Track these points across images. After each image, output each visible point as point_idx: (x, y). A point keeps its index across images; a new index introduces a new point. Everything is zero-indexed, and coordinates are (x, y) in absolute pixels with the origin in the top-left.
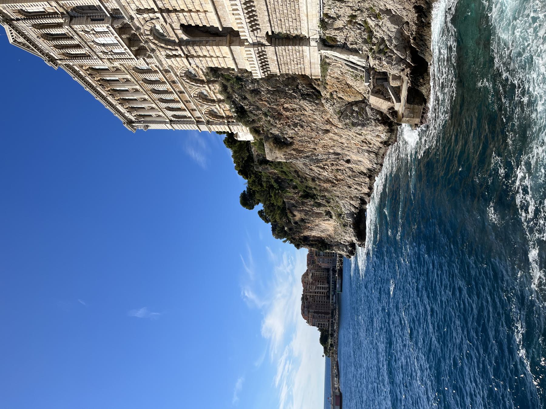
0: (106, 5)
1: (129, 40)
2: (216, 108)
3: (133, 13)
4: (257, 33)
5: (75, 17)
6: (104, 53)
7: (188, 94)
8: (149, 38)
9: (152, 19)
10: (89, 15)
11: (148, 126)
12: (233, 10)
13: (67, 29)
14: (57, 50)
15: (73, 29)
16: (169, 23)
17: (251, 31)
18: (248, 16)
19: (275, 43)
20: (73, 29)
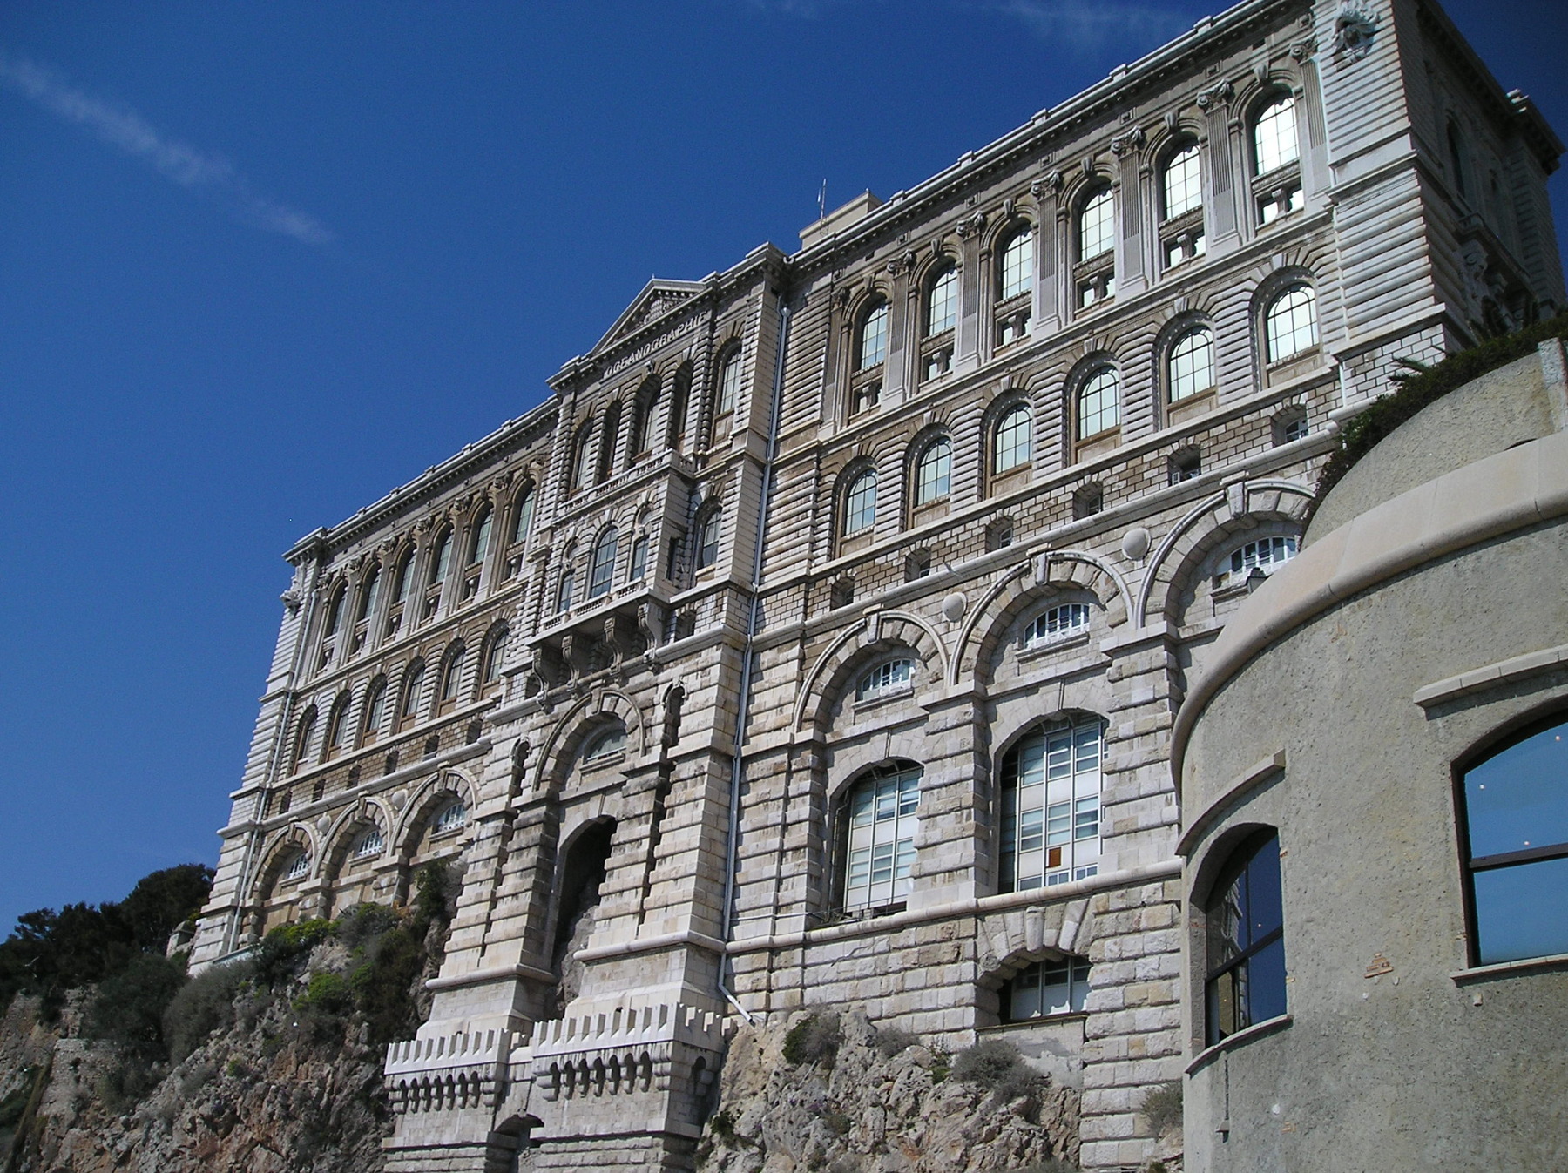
2: (304, 879)
3: (672, 673)
4: (545, 1087)
6: (572, 544)
7: (379, 784)
8: (590, 701)
9: (648, 728)
10: (690, 537)
11: (295, 608)
12: (632, 1013)
13: (660, 459)
14: (606, 405)
15: (658, 476)
16: (624, 783)
17: (554, 1065)
18: (605, 1062)
19: (499, 1147)
20: (658, 476)
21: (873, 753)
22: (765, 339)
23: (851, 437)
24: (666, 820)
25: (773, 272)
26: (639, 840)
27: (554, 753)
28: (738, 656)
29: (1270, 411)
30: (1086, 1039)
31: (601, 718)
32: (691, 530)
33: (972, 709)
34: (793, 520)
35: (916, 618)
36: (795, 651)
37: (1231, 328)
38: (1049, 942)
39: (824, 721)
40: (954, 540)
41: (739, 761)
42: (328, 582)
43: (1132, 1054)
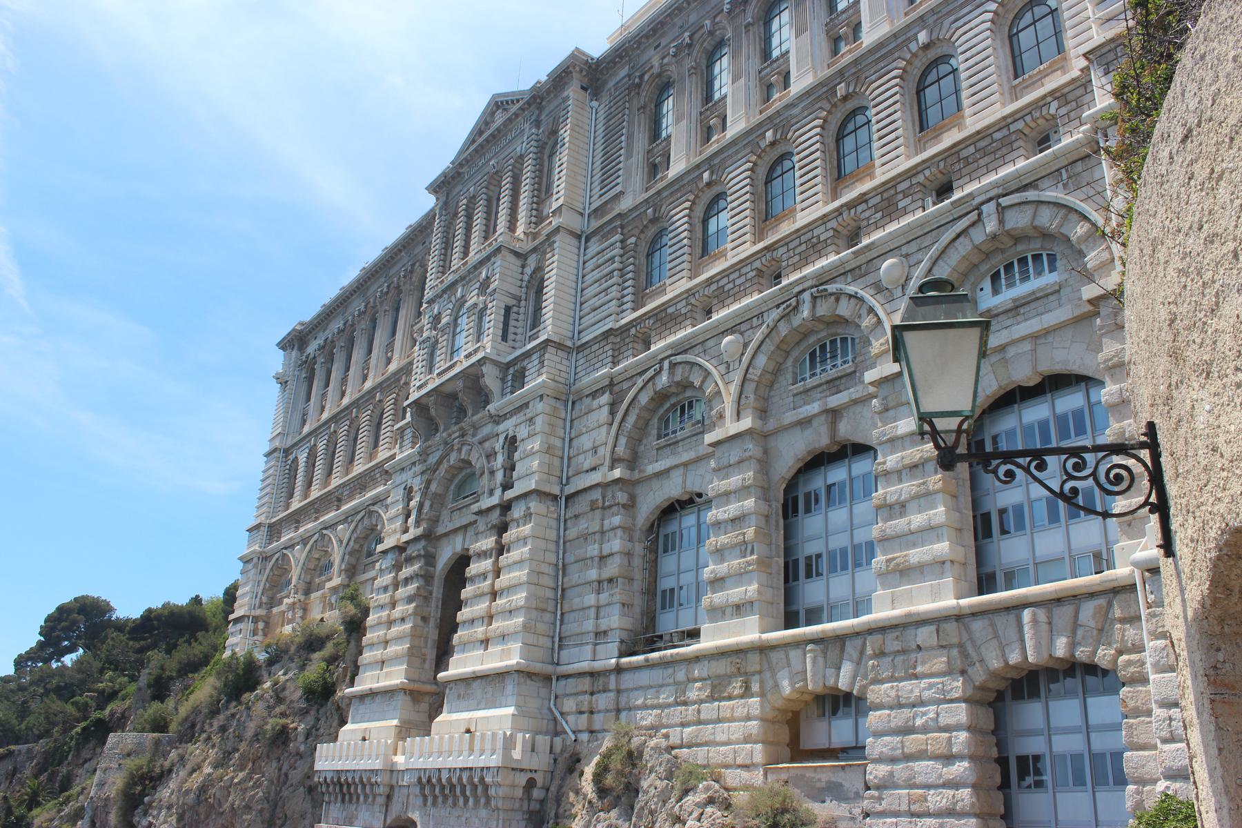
0: (535, 356)
1: (453, 396)
3: (508, 426)
5: (523, 267)
8: (452, 450)
9: (492, 473)
10: (523, 303)
16: (475, 522)
17: (420, 778)
18: (454, 780)
21: (672, 489)
22: (578, 129)
23: (646, 201)
24: (505, 555)
25: (581, 71)
26: (484, 576)
27: (429, 496)
28: (559, 405)
29: (1020, 125)
30: (868, 788)
31: (461, 465)
32: (523, 297)
33: (751, 446)
34: (603, 280)
35: (700, 360)
36: (605, 398)
37: (974, 51)
38: (831, 682)
39: (633, 461)
40: (731, 286)
41: (563, 499)
42: (306, 362)
43: (915, 808)
